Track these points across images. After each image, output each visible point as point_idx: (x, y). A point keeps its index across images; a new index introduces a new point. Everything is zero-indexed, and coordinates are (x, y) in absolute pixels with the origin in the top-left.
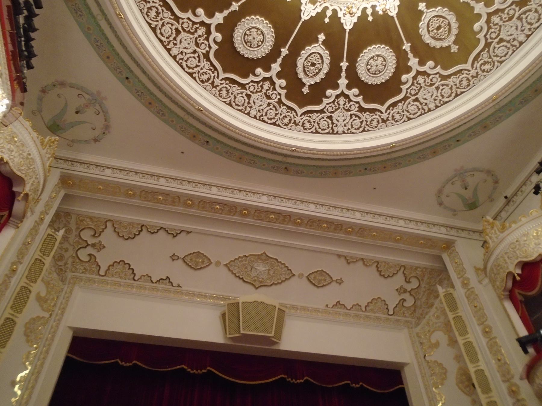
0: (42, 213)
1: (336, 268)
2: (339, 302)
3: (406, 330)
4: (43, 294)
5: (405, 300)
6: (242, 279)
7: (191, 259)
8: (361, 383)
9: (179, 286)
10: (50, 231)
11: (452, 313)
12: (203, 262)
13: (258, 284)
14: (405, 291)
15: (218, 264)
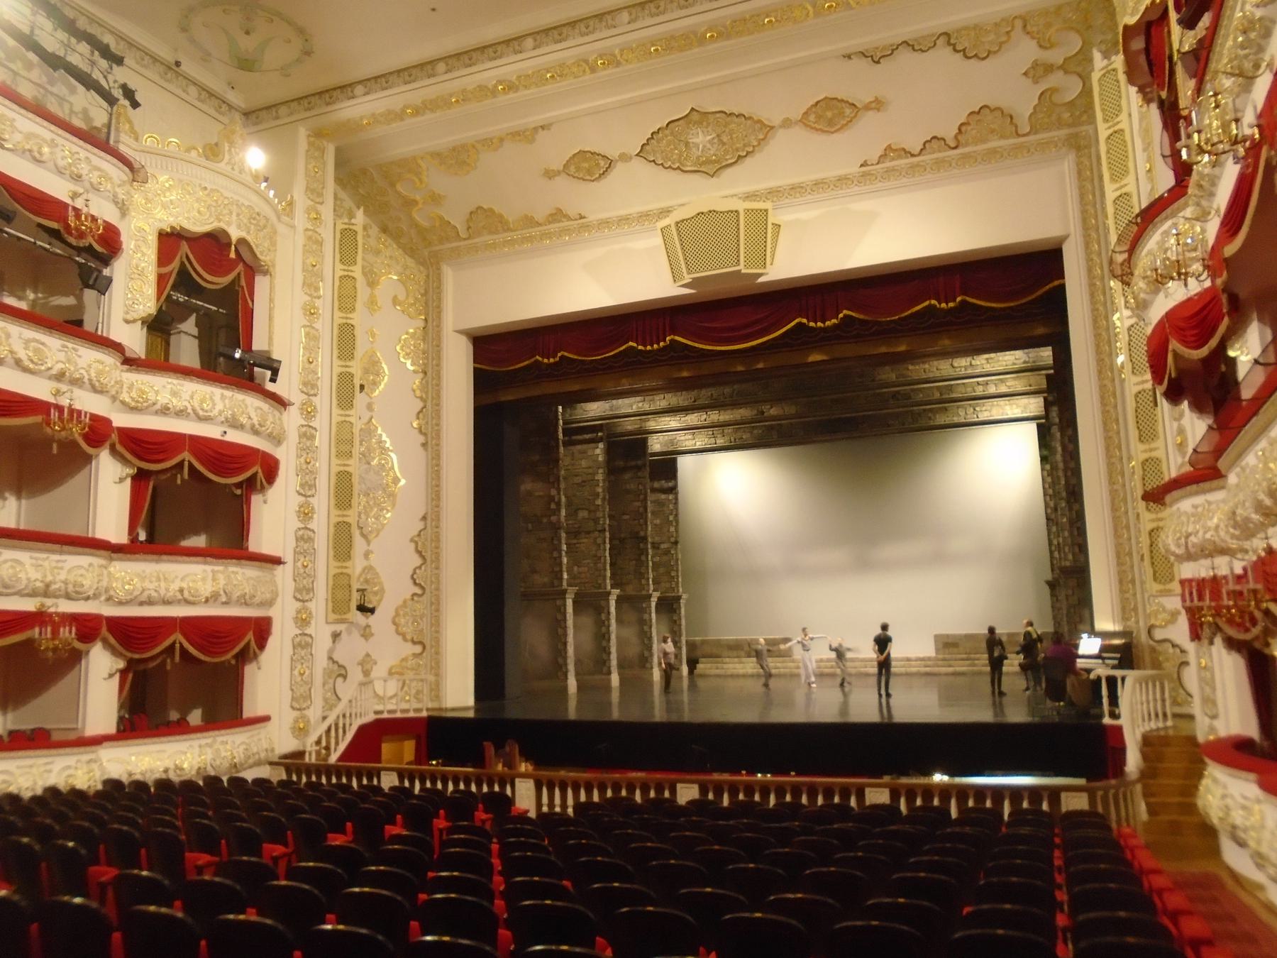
0: (308, 211)
1: (856, 83)
2: (889, 146)
3: (1072, 157)
4: (401, 297)
5: (1053, 90)
6: (678, 168)
7: (578, 169)
8: (959, 299)
9: (582, 217)
10: (340, 226)
11: (1107, 125)
12: (598, 164)
13: (712, 167)
14: (1049, 69)
15: (624, 158)
